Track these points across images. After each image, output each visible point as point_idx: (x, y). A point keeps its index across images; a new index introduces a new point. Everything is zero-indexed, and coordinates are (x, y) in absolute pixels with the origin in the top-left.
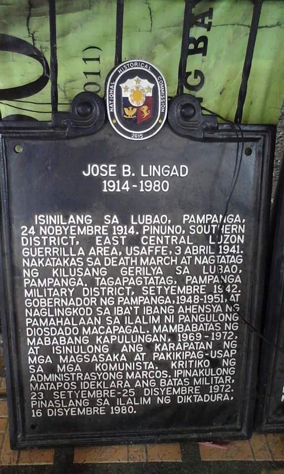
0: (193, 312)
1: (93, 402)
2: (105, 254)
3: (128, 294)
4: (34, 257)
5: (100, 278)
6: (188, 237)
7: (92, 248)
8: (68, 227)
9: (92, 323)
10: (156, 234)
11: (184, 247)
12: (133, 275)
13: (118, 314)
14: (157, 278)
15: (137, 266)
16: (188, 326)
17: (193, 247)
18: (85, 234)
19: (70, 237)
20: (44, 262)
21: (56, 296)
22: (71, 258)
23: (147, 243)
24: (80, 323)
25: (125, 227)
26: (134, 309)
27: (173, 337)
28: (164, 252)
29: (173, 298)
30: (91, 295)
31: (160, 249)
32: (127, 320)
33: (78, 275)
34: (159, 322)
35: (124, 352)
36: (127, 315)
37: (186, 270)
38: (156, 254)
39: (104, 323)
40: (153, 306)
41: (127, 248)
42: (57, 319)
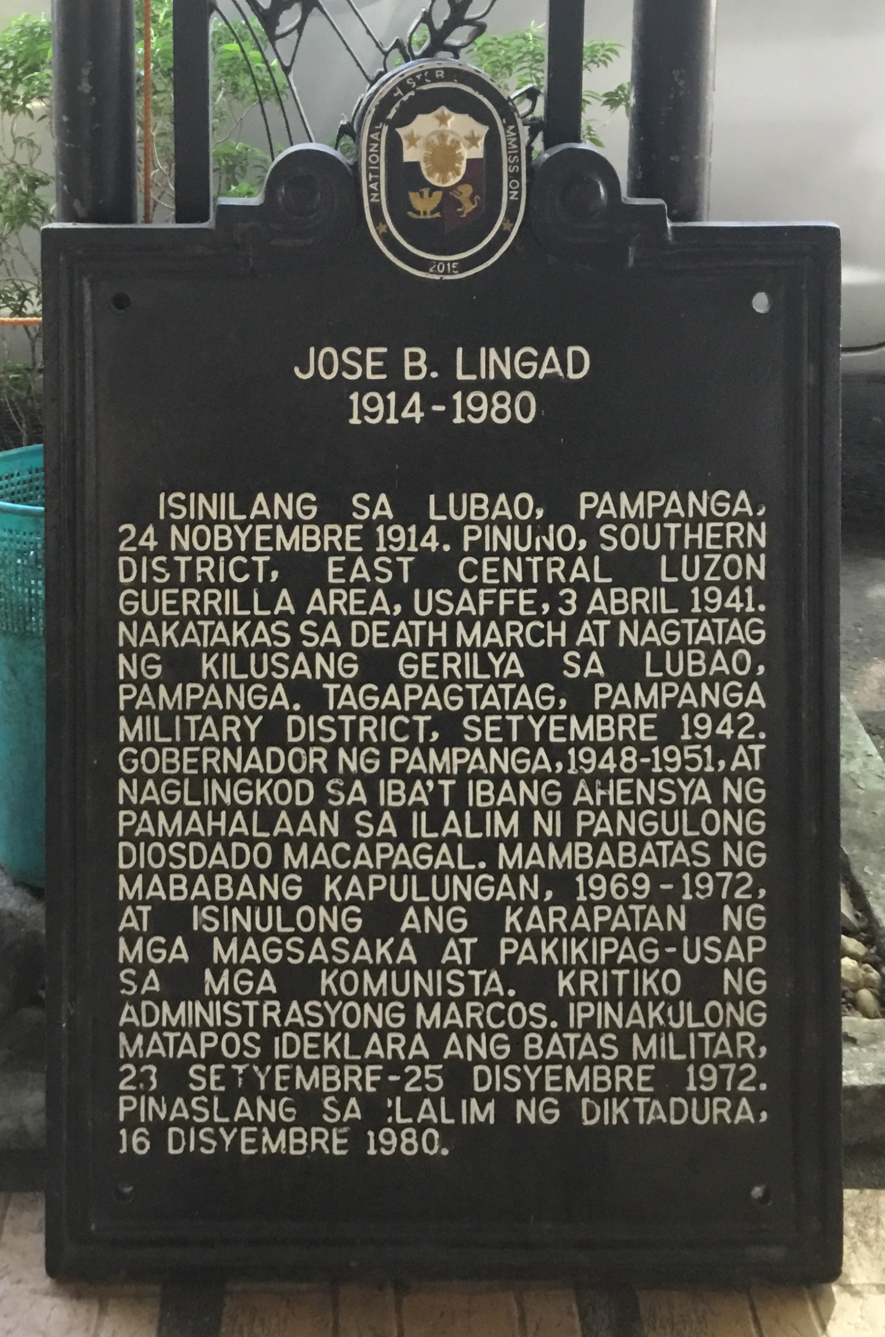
0: (620, 802)
2: (353, 612)
3: (421, 739)
4: (151, 619)
5: (338, 686)
6: (597, 559)
7: (318, 593)
8: (250, 527)
9: (312, 829)
10: (501, 552)
11: (585, 590)
12: (436, 677)
13: (391, 803)
14: (507, 687)
15: (447, 650)
16: (605, 847)
17: (613, 591)
18: (297, 548)
19: (254, 558)
20: (179, 634)
21: (209, 742)
22: (255, 620)
23: (475, 578)
24: (277, 830)
25: (413, 529)
26: (439, 789)
27: (561, 885)
28: (527, 608)
29: (557, 753)
30: (312, 739)
31: (515, 597)
32: (419, 824)
33: (274, 674)
34: (516, 835)
35: (410, 933)
36: (419, 806)
37: (595, 666)
38: (502, 612)
39: (349, 831)
41: (417, 592)
42: (210, 813)
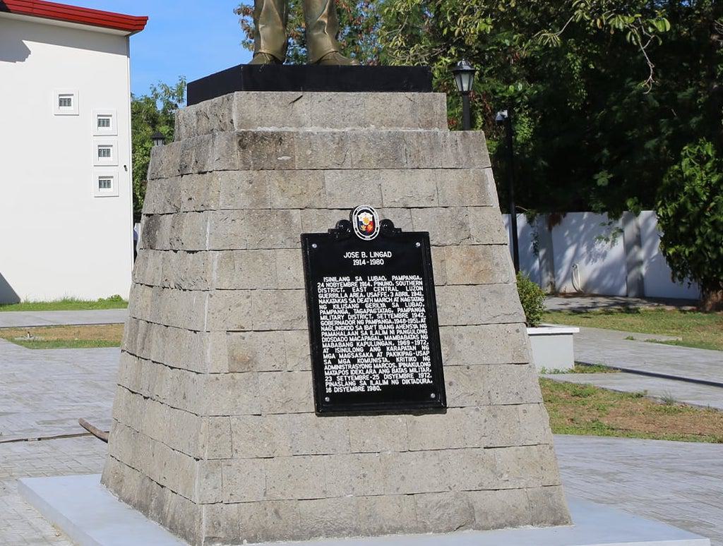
1: (358, 383)
29: (393, 320)
32: (371, 332)
39: (360, 334)
40: (383, 324)
